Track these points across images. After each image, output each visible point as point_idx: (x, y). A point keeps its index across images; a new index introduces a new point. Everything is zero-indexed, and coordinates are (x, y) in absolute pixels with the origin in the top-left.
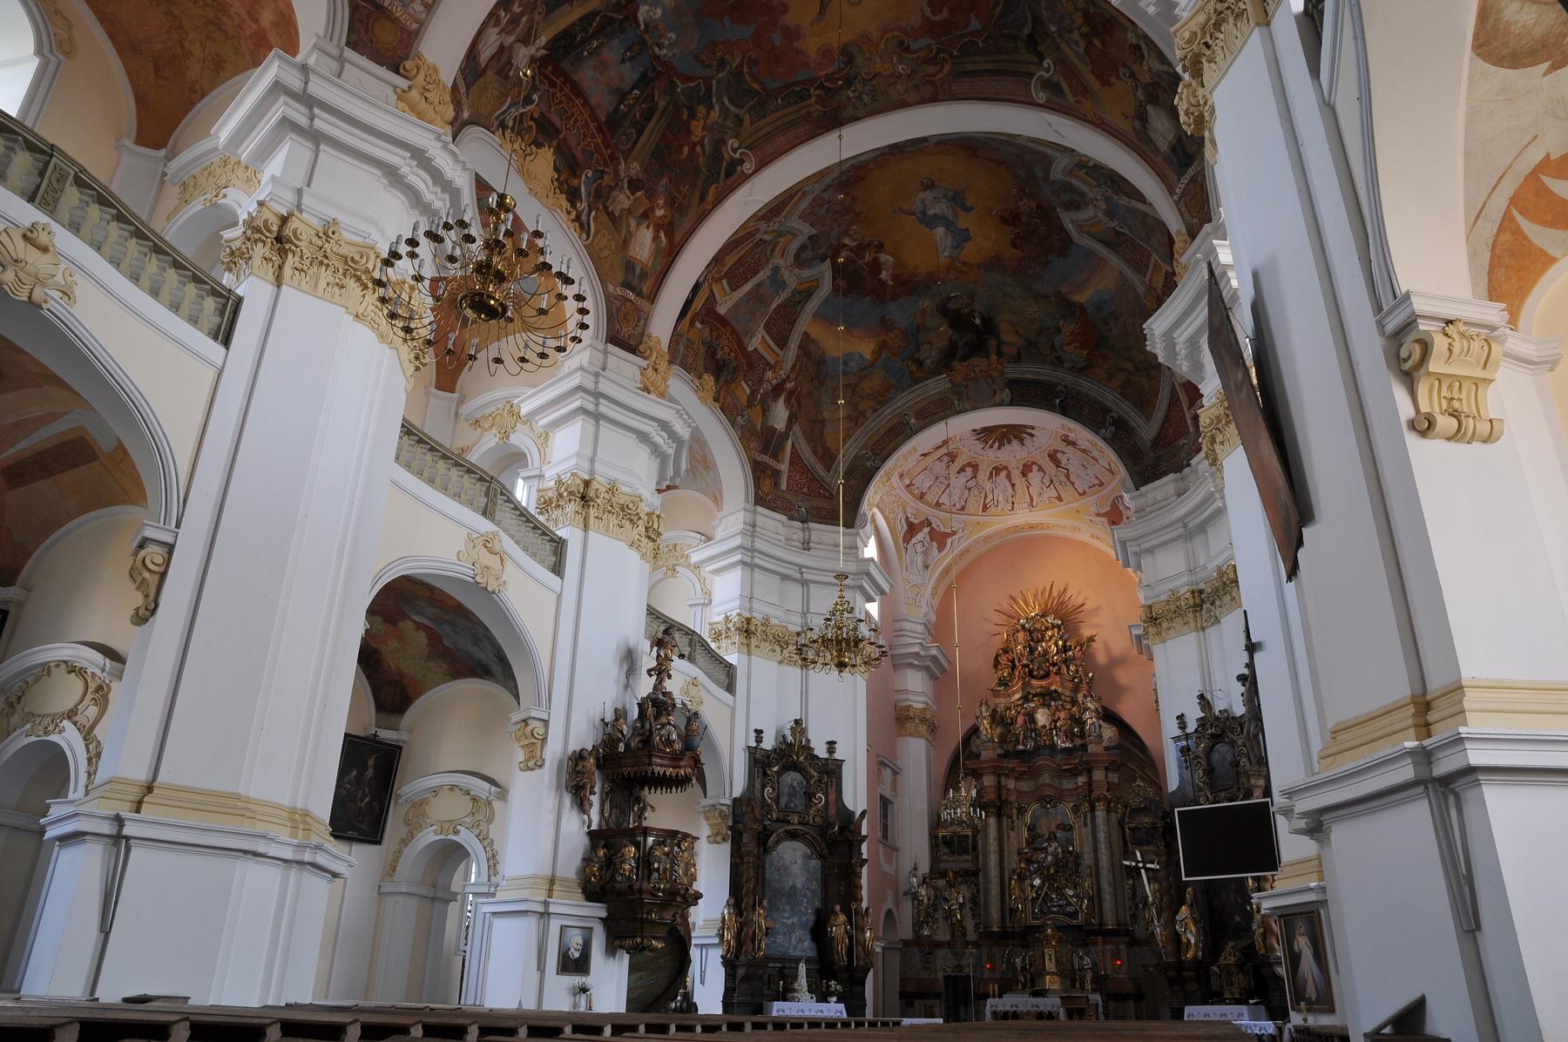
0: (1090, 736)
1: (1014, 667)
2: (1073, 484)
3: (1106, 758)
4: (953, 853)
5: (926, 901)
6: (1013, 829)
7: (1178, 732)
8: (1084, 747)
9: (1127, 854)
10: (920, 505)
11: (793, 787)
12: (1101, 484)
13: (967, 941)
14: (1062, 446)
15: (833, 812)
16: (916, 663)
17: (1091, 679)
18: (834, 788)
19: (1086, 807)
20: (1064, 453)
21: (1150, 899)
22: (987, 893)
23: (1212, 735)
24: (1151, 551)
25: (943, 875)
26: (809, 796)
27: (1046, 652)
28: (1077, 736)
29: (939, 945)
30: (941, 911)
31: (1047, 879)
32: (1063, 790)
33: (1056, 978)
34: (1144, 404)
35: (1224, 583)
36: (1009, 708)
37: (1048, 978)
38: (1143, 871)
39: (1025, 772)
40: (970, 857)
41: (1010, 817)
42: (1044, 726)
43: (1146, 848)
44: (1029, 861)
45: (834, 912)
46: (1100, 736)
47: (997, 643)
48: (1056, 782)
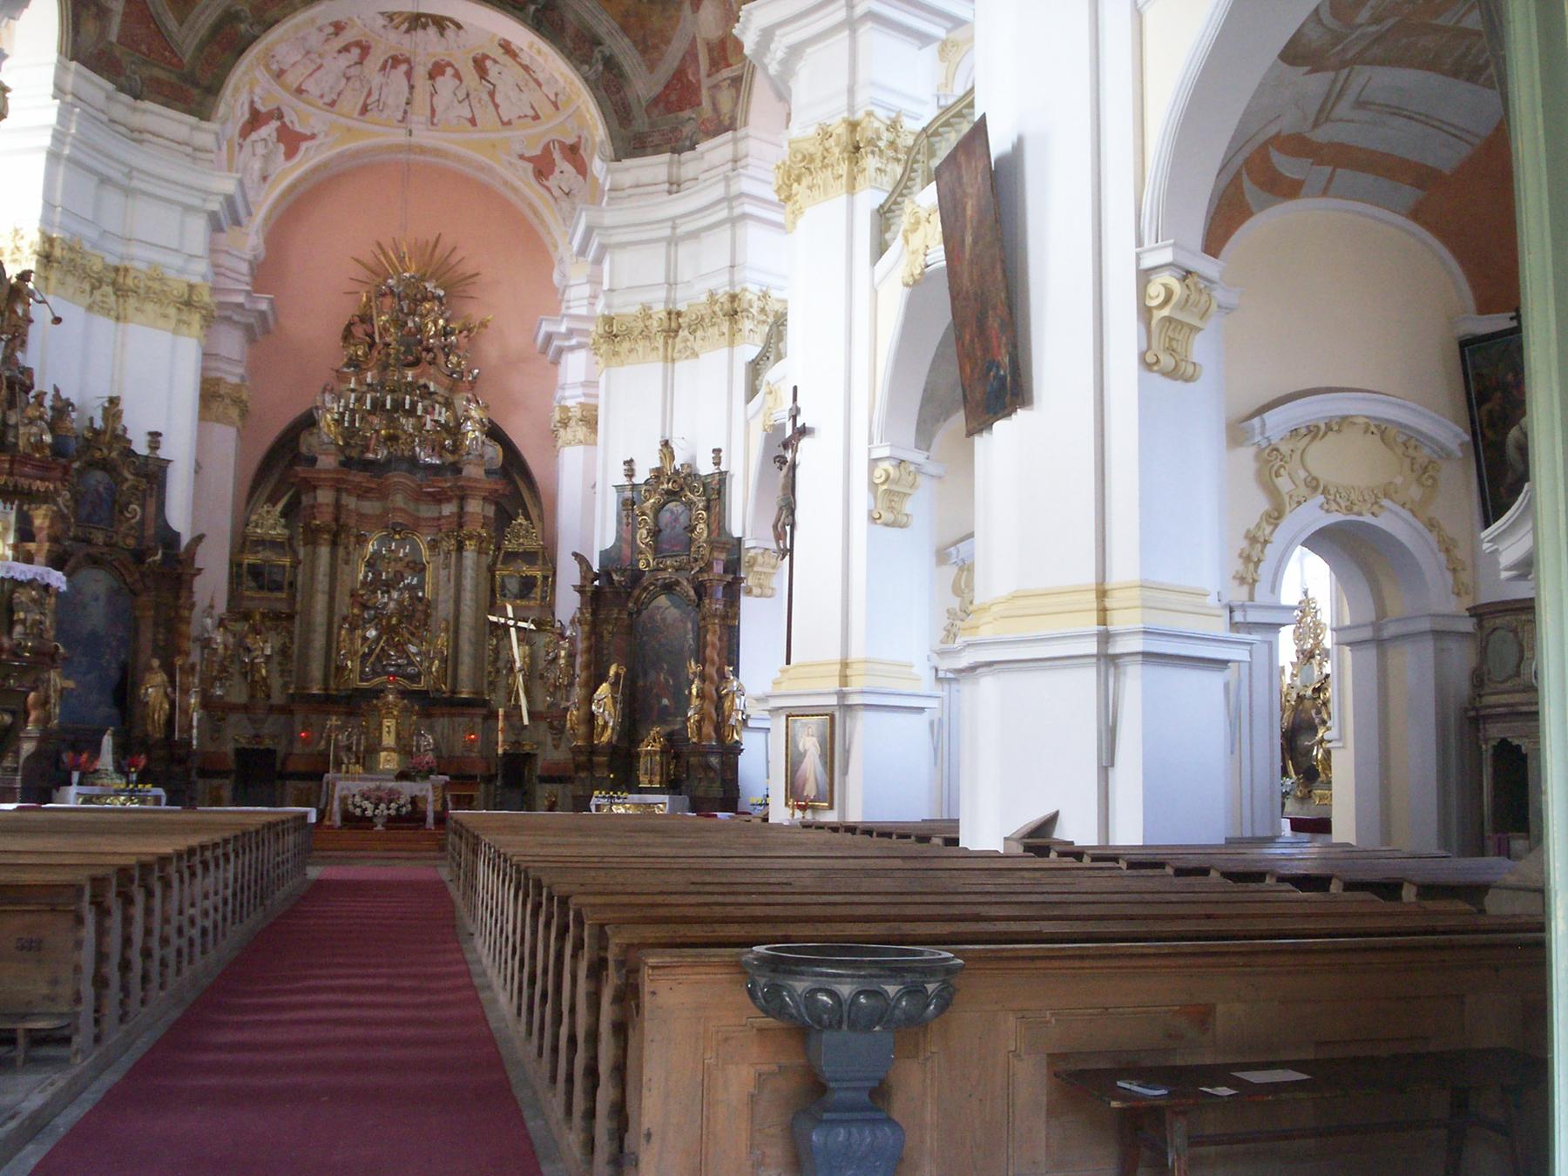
0: (468, 454)
1: (372, 345)
2: (496, 106)
3: (487, 486)
4: (261, 588)
5: (221, 649)
6: (347, 563)
7: (624, 481)
8: (456, 469)
9: (494, 608)
10: (275, 87)
12: (536, 117)
14: (497, 53)
17: (475, 378)
19: (451, 544)
20: (495, 62)
21: (518, 665)
22: (306, 643)
23: (668, 492)
24: (622, 246)
25: (246, 616)
27: (420, 329)
28: (448, 450)
29: (234, 708)
31: (388, 631)
33: (393, 754)
34: (649, 46)
35: (714, 313)
37: (383, 754)
38: (513, 630)
39: (372, 489)
40: (284, 595)
41: (346, 548)
44: (365, 607)
45: (150, 669)
46: (482, 456)
47: (347, 310)
48: (411, 507)
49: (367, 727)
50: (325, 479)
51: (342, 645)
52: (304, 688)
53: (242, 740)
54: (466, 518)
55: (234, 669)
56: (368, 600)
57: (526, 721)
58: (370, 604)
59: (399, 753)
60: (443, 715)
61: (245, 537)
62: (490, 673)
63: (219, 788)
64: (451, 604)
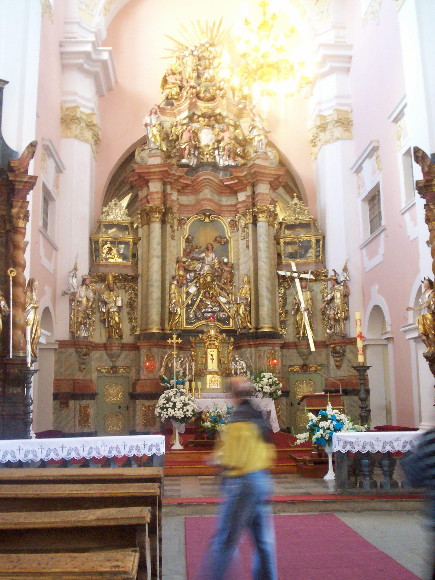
6: (173, 238)
13: (123, 344)
16: (86, 66)
21: (303, 306)
22: (147, 296)
25: (102, 279)
28: (239, 156)
29: (96, 347)
30: (98, 315)
32: (222, 206)
33: (218, 378)
37: (209, 377)
38: (297, 281)
40: (130, 263)
41: (172, 227)
42: (208, 146)
44: (187, 271)
48: (216, 198)
49: (196, 356)
50: (154, 173)
51: (173, 296)
52: (146, 330)
53: (103, 370)
54: (257, 199)
55: (95, 318)
56: (189, 265)
57: (313, 348)
58: (191, 268)
59: (222, 375)
60: (250, 346)
61: (100, 223)
62: (280, 314)
63: (87, 407)
64: (251, 264)
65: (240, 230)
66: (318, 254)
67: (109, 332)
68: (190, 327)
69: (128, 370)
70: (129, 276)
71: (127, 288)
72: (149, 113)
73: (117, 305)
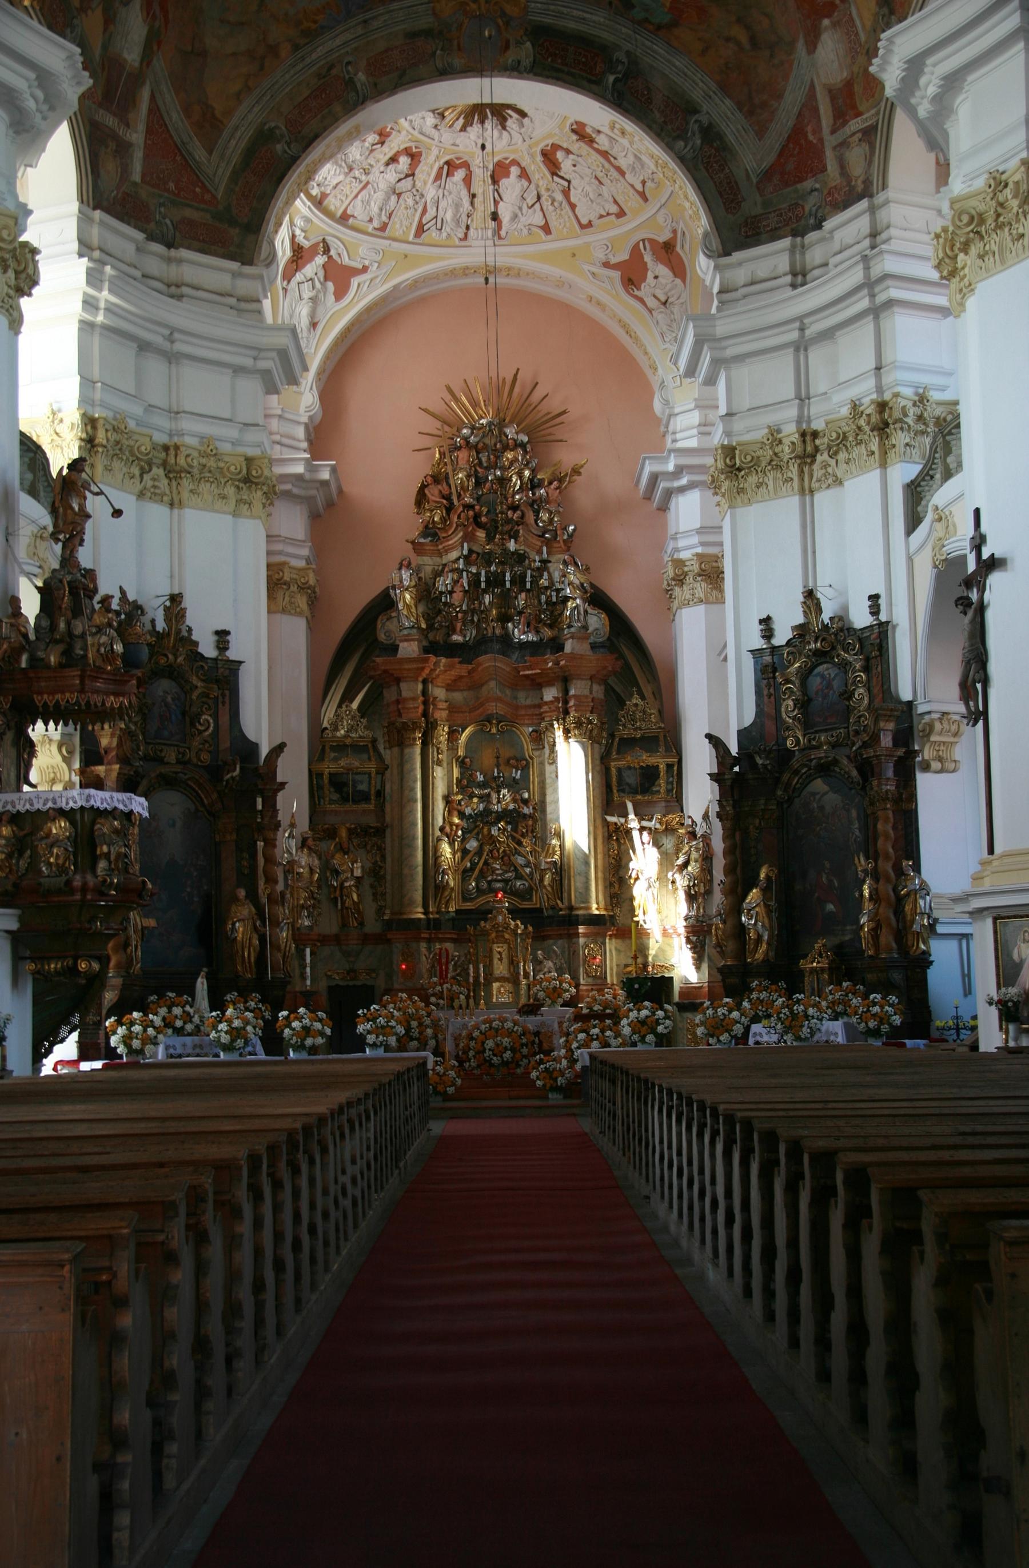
0: (570, 626)
1: (449, 509)
2: (573, 207)
4: (345, 799)
7: (759, 643)
8: (556, 646)
11: (167, 705)
12: (621, 214)
14: (570, 141)
15: (225, 744)
16: (295, 491)
17: (571, 536)
18: (227, 705)
20: (568, 152)
23: (817, 653)
24: (740, 358)
25: (331, 833)
26: (189, 719)
27: (503, 481)
35: (859, 428)
36: (438, 574)
37: (496, 985)
40: (372, 807)
43: (639, 797)
45: (236, 899)
46: (585, 627)
52: (401, 914)
60: (560, 937)
65: (547, 746)
66: (670, 787)
67: (343, 917)
68: (469, 906)
69: (374, 975)
70: (371, 828)
71: (369, 847)
72: (398, 566)
73: (355, 874)
